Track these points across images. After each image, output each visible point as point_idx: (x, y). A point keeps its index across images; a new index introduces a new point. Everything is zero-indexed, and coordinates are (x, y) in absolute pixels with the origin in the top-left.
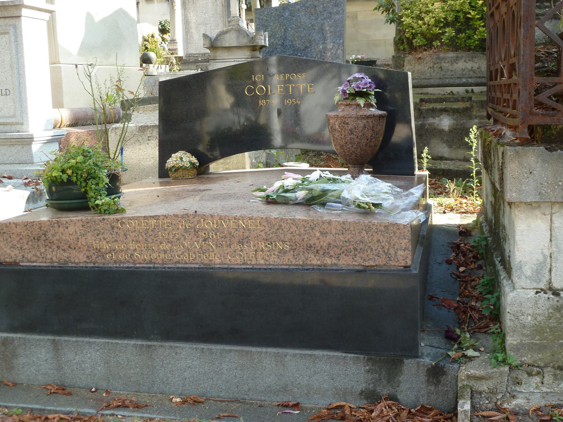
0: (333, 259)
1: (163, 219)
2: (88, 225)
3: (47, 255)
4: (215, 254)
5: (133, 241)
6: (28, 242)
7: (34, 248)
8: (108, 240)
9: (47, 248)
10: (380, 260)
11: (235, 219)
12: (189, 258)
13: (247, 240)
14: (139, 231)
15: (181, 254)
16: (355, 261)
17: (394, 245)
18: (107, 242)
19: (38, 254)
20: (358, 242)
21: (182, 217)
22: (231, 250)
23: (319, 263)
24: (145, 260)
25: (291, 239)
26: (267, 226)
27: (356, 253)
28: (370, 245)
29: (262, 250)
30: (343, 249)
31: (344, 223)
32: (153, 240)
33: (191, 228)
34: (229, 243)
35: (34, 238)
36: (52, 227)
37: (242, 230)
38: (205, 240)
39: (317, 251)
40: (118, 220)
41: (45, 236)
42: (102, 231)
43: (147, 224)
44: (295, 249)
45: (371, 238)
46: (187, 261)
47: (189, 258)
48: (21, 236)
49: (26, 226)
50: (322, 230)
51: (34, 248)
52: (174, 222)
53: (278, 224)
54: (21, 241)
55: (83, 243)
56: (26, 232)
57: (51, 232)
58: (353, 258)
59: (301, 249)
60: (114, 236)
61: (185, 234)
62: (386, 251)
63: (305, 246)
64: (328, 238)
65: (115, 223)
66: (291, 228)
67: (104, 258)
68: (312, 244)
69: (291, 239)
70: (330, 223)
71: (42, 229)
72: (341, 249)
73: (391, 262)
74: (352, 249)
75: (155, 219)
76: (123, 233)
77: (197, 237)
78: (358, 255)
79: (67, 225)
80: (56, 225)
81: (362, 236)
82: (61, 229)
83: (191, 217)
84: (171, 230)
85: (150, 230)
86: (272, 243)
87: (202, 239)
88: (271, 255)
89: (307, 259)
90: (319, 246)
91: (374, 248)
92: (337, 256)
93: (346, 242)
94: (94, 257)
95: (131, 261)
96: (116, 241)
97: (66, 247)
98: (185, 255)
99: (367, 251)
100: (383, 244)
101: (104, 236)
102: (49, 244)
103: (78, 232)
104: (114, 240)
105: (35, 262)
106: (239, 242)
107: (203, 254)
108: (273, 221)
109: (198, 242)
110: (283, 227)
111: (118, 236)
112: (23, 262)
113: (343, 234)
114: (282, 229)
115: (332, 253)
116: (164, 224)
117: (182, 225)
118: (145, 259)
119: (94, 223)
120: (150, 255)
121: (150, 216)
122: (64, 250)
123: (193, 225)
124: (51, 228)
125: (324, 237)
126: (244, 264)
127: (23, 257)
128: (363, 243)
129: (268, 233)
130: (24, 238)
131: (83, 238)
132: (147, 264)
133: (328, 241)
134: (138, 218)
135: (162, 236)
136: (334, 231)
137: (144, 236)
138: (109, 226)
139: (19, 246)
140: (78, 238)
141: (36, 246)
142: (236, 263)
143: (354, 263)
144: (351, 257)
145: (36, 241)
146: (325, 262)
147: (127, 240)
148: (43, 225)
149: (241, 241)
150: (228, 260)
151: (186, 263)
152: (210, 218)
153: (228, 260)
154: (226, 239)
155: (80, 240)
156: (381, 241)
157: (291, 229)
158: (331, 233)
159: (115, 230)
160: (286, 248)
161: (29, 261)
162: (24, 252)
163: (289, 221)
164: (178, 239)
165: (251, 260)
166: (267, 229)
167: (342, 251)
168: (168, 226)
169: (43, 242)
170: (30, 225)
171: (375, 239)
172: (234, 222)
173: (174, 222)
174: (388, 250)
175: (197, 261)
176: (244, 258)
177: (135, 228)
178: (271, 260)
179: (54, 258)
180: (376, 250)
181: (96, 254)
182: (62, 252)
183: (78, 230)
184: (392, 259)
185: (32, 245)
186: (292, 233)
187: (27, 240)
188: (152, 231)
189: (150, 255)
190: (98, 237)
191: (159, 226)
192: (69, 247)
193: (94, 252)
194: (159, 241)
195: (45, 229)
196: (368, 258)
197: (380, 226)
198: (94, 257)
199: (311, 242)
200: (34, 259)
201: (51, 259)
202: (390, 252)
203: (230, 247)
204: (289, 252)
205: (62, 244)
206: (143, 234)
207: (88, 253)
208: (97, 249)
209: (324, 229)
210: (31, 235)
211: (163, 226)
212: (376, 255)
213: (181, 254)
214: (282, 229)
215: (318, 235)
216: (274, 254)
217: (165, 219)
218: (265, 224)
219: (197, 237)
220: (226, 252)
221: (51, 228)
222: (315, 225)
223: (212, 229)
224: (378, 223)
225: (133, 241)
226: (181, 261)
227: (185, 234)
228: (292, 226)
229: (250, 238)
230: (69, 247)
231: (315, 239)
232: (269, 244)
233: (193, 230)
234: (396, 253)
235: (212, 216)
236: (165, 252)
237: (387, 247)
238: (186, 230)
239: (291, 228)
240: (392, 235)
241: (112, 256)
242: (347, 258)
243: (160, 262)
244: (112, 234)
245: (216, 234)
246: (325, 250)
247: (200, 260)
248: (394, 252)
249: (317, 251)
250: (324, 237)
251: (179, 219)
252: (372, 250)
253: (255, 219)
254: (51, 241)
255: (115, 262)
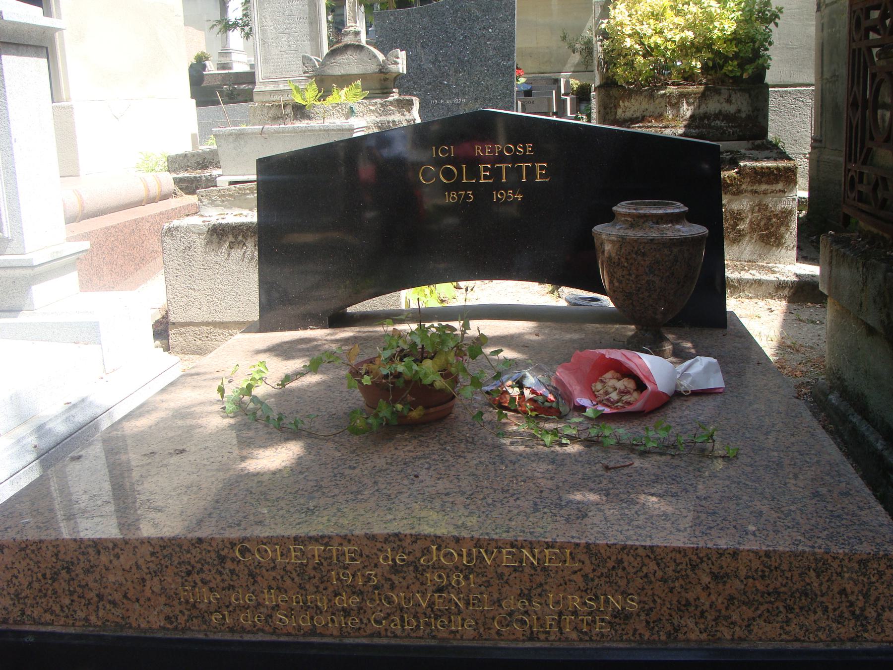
0: (737, 629)
1: (341, 544)
2: (165, 552)
3: (75, 611)
4: (463, 620)
5: (270, 588)
6: (30, 584)
7: (45, 595)
8: (212, 585)
9: (75, 597)
10: (843, 630)
11: (512, 546)
12: (403, 626)
13: (539, 590)
14: (284, 569)
15: (384, 618)
16: (786, 633)
17: (878, 599)
18: (211, 590)
19: (57, 609)
20: (797, 595)
21: (387, 539)
22: (501, 610)
23: (704, 636)
24: (300, 628)
25: (643, 589)
26: (587, 562)
27: (790, 616)
28: (824, 599)
29: (575, 613)
30: (762, 608)
31: (767, 554)
32: (317, 587)
33: (409, 564)
34: (496, 596)
35: (44, 576)
36: (83, 553)
37: (528, 570)
38: (440, 590)
39: (702, 613)
40: (233, 544)
41: (68, 572)
42: (199, 566)
43: (303, 553)
44: (651, 609)
45: (825, 585)
46: (399, 633)
47: (403, 626)
48: (16, 572)
49: (23, 549)
50: (715, 570)
51: (45, 595)
52: (366, 551)
53: (614, 558)
54: (14, 580)
55: (154, 589)
56: (24, 563)
57: (82, 565)
58: (782, 628)
59: (665, 608)
60: (225, 577)
61: (393, 577)
62: (858, 612)
63: (674, 602)
64: (728, 586)
65: (226, 550)
66: (644, 565)
67: (205, 622)
68: (691, 600)
69: (643, 589)
70: (735, 554)
71: (61, 556)
72: (757, 609)
73: (866, 635)
74: (782, 609)
75: (322, 545)
76: (246, 572)
77: (422, 584)
78: (795, 621)
79: (117, 550)
80: (91, 550)
81: (807, 580)
82: (104, 559)
83: (409, 541)
84: (360, 567)
85: (310, 566)
86: (597, 598)
87: (435, 588)
88: (594, 621)
89: (677, 630)
90: (708, 604)
91: (831, 607)
92: (746, 623)
93: (769, 594)
94: (182, 619)
95: (267, 628)
96: (231, 587)
97: (117, 596)
98: (393, 621)
99: (815, 613)
100: (852, 598)
101: (204, 576)
102: (80, 590)
103: (144, 567)
104: (226, 584)
105: (52, 624)
106: (521, 595)
107: (436, 619)
108: (602, 551)
109: (424, 595)
110: (626, 564)
111: (235, 577)
112: (24, 623)
113: (763, 577)
114: (624, 569)
115: (735, 617)
116: (344, 554)
117: (386, 558)
118: (299, 626)
119: (178, 549)
120: (312, 618)
121: (310, 538)
122: (114, 603)
123: (412, 558)
124: (81, 557)
125: (720, 586)
126: (531, 638)
127: (23, 614)
128: (806, 595)
129: (591, 576)
130: (21, 575)
131: (156, 579)
132: (304, 635)
133: (727, 592)
134: (281, 541)
135: (338, 579)
136: (743, 573)
137: (297, 579)
138: (214, 555)
139: (12, 591)
140: (144, 580)
141: (50, 592)
142: (512, 637)
143: (784, 636)
144: (778, 625)
145: (50, 582)
146: (719, 635)
147: (256, 587)
148: (63, 550)
149: (526, 592)
150: (493, 632)
151: (396, 636)
152: (453, 544)
153: (493, 632)
154: (490, 589)
155: (148, 583)
156: (849, 591)
157: (645, 569)
158: (737, 577)
159: (229, 565)
160: (631, 606)
161: (35, 622)
162: (25, 604)
163: (641, 551)
164: (376, 587)
165: (548, 633)
166: (588, 568)
167: (759, 612)
168: (352, 559)
169: (64, 585)
170: (34, 547)
171: (836, 588)
172: (509, 553)
173: (366, 551)
174: (863, 609)
175: (421, 633)
176: (531, 627)
177: (274, 560)
178: (593, 633)
179: (93, 618)
180: (835, 610)
181: (187, 613)
182: (108, 606)
183: (141, 562)
184: (870, 628)
185: (40, 591)
186: (646, 576)
187: (29, 579)
188: (315, 568)
189: (312, 618)
190: (190, 579)
191: (331, 558)
192: (125, 596)
193: (183, 608)
194: (330, 589)
195: (68, 559)
196: (815, 627)
197: (850, 560)
198: (182, 619)
199: (691, 596)
200: (48, 617)
201: (87, 619)
202: (867, 613)
203: (500, 606)
204: (638, 615)
205: (108, 591)
206: (294, 575)
207: (167, 610)
208: (187, 602)
209: (722, 568)
210: (36, 570)
211: (341, 558)
212: (834, 621)
213: (384, 618)
214: (624, 569)
215: (706, 579)
216: (602, 620)
217: (345, 543)
218: (585, 557)
219: (422, 584)
220: (490, 615)
221: (81, 557)
222: (701, 559)
223: (457, 568)
224: (845, 554)
225: (270, 588)
226: (383, 633)
227: (393, 577)
228: (647, 561)
229: (547, 587)
230: (125, 596)
231: (699, 589)
232: (590, 599)
233: (411, 568)
234: (879, 615)
235: (457, 540)
236: (346, 612)
237: (860, 604)
238: (395, 569)
239: (644, 565)
240: (873, 579)
241: (224, 618)
242: (768, 627)
243: (335, 633)
244: (221, 573)
245: (466, 578)
246: (720, 611)
247: (428, 631)
248: (875, 615)
249: (702, 613)
250: (720, 586)
251: (379, 545)
252: (826, 609)
253: (562, 547)
254: (83, 583)
255: (231, 630)
